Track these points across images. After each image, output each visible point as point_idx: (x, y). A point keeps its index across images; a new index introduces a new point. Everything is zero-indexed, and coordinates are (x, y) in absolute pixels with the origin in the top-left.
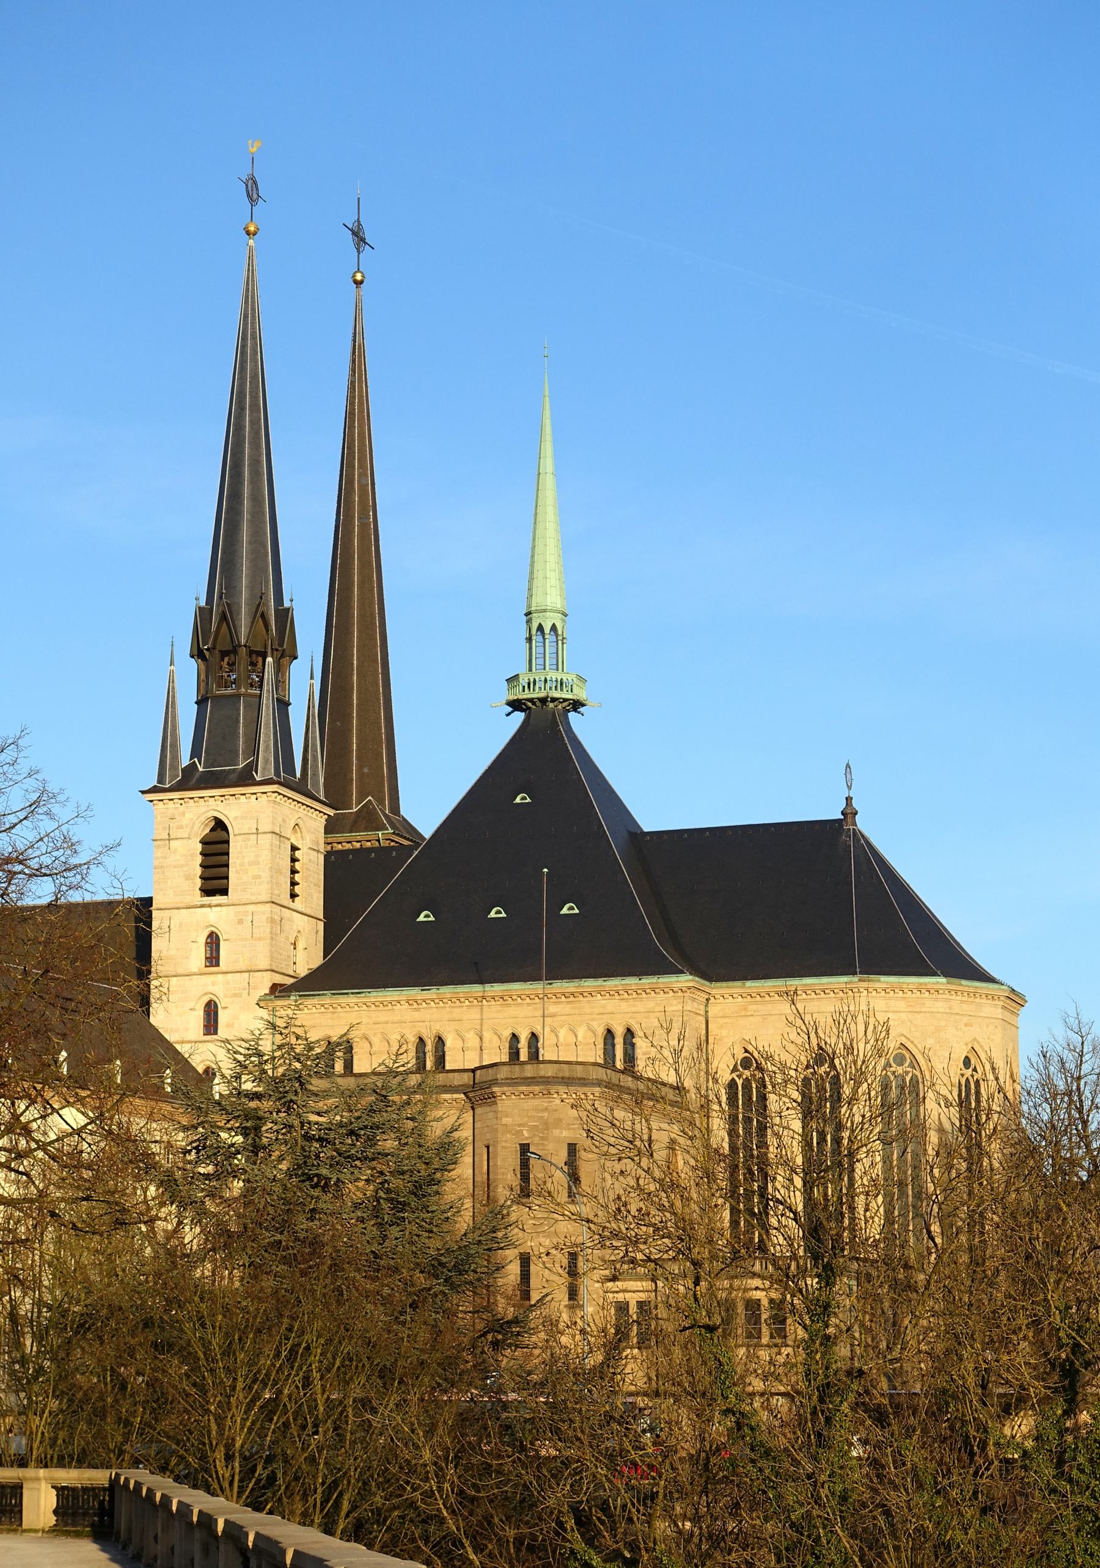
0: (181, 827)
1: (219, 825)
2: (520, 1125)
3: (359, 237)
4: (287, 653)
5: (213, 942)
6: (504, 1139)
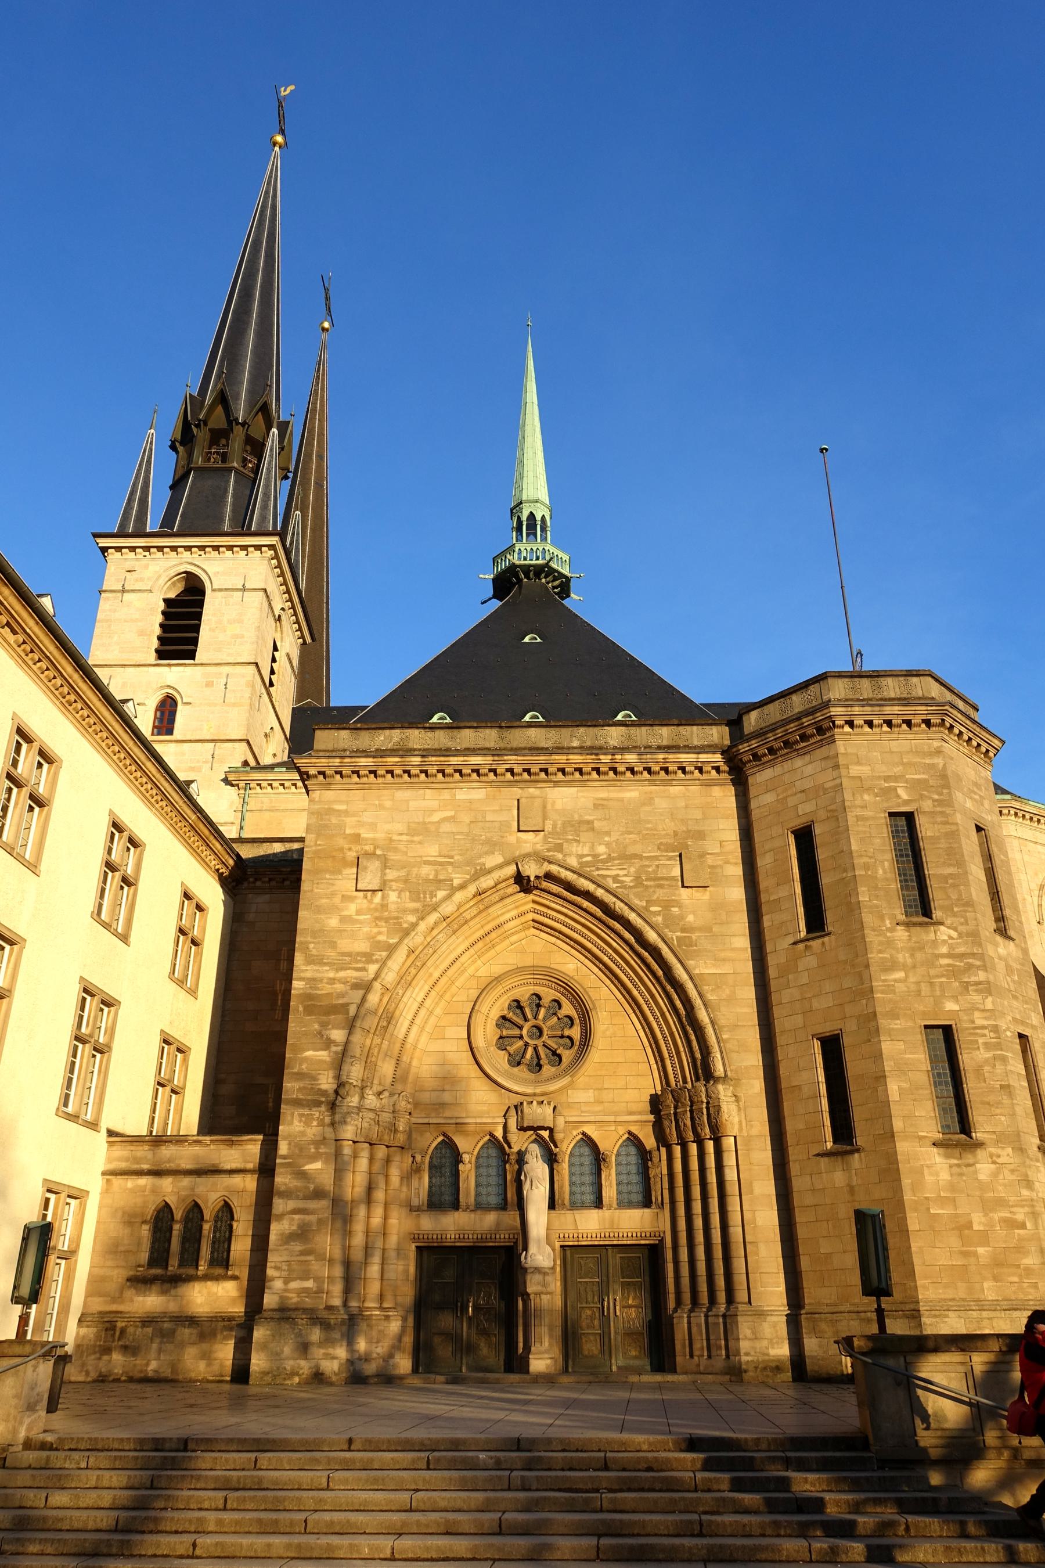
0: (142, 580)
2: (887, 779)
6: (858, 802)
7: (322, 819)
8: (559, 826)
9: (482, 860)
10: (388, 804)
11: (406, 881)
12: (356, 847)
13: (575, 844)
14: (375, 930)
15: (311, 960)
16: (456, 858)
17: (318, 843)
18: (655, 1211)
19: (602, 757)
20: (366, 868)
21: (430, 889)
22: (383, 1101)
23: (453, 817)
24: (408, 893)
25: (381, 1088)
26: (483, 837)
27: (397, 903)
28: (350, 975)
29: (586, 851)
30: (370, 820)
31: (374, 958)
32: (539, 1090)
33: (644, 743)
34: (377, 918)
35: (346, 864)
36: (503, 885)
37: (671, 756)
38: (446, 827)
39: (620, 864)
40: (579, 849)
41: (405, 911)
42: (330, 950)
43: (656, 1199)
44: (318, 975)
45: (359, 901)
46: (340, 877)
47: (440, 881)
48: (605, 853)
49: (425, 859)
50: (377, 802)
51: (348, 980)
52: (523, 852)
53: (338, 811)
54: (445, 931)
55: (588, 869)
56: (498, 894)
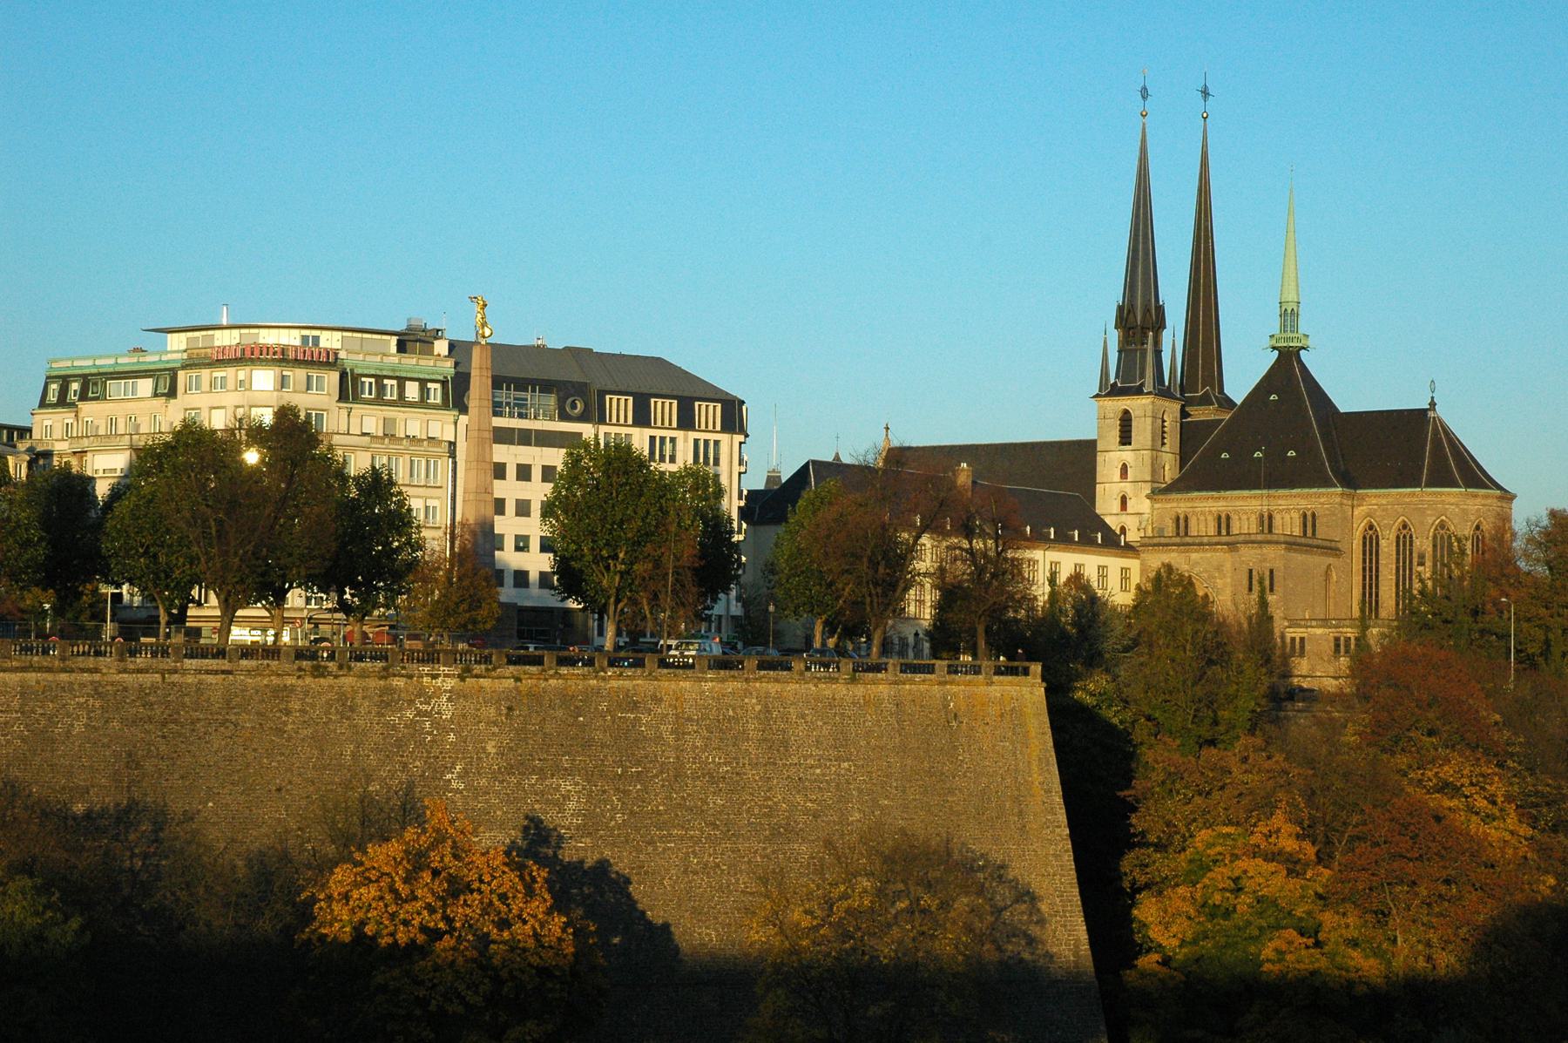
1: (1126, 412)
3: (1205, 93)
4: (1159, 324)
5: (1124, 469)
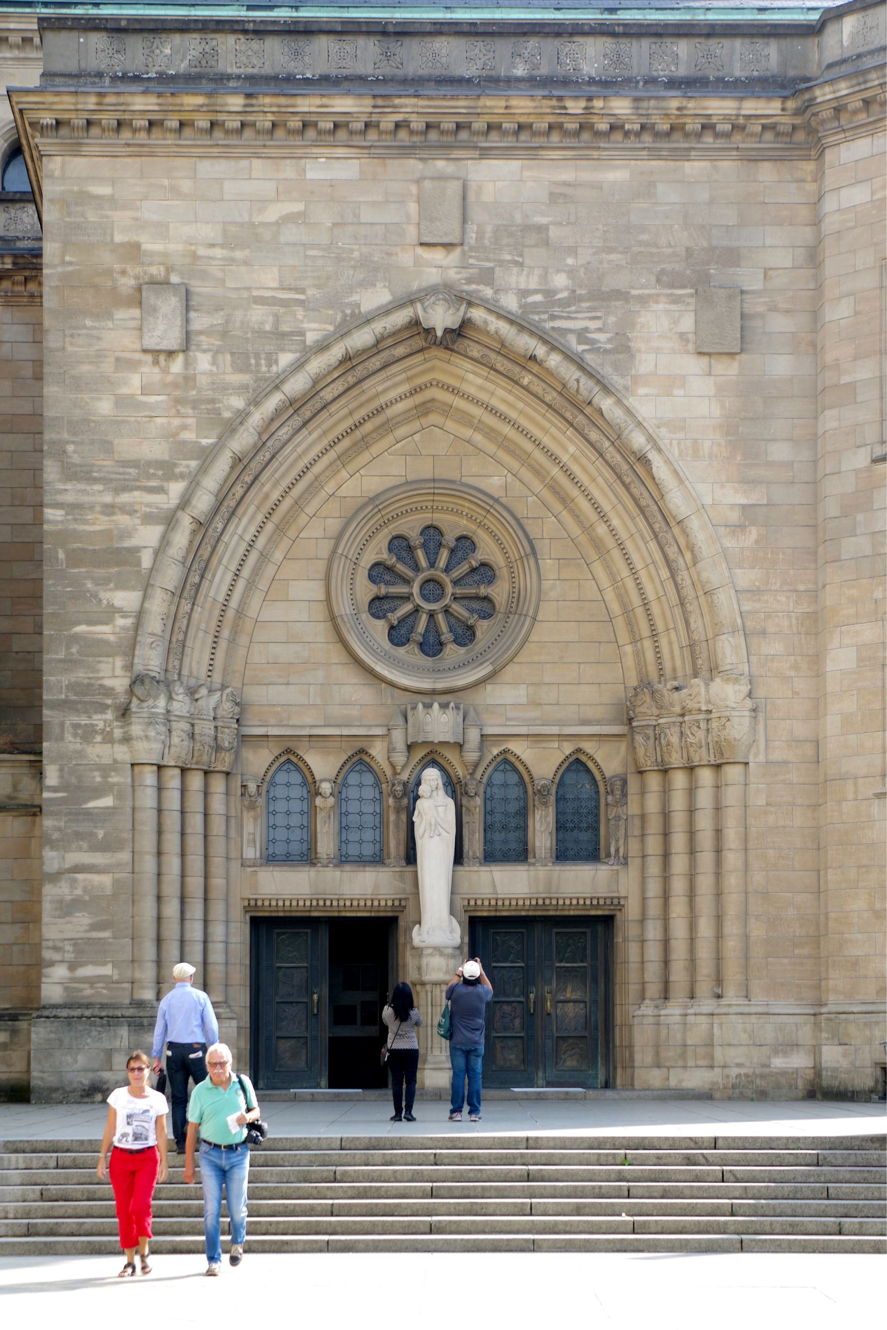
7: (69, 214)
8: (488, 235)
9: (355, 298)
10: (186, 185)
11: (224, 334)
12: (134, 270)
13: (515, 270)
14: (177, 422)
15: (72, 473)
16: (310, 292)
17: (67, 258)
18: (614, 868)
19: (569, 103)
20: (155, 310)
21: (268, 348)
22: (199, 702)
23: (302, 214)
24: (228, 357)
25: (192, 682)
26: (356, 254)
27: (211, 373)
28: (139, 500)
29: (533, 284)
30: (155, 218)
31: (177, 470)
32: (440, 685)
33: (644, 71)
34: (178, 401)
35: (119, 300)
36: (389, 342)
37: (691, 104)
38: (290, 234)
39: (591, 309)
40: (522, 279)
41: (224, 388)
42: (102, 456)
43: (617, 851)
44: (85, 499)
45: (146, 369)
46: (110, 324)
47: (283, 335)
48: (566, 288)
49: (255, 293)
50: (166, 182)
51: (137, 507)
52: (424, 284)
53: (98, 197)
54: (290, 423)
55: (536, 318)
56: (379, 357)
